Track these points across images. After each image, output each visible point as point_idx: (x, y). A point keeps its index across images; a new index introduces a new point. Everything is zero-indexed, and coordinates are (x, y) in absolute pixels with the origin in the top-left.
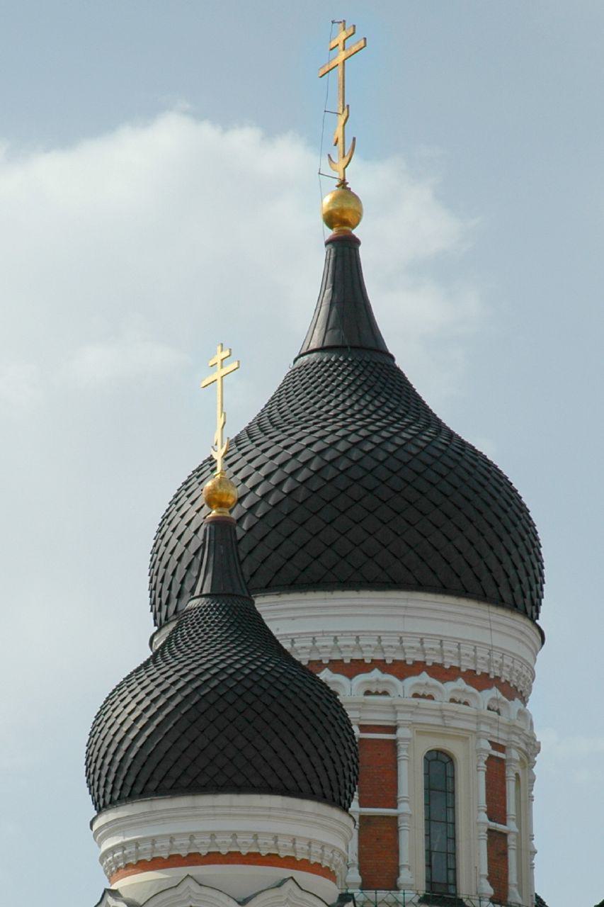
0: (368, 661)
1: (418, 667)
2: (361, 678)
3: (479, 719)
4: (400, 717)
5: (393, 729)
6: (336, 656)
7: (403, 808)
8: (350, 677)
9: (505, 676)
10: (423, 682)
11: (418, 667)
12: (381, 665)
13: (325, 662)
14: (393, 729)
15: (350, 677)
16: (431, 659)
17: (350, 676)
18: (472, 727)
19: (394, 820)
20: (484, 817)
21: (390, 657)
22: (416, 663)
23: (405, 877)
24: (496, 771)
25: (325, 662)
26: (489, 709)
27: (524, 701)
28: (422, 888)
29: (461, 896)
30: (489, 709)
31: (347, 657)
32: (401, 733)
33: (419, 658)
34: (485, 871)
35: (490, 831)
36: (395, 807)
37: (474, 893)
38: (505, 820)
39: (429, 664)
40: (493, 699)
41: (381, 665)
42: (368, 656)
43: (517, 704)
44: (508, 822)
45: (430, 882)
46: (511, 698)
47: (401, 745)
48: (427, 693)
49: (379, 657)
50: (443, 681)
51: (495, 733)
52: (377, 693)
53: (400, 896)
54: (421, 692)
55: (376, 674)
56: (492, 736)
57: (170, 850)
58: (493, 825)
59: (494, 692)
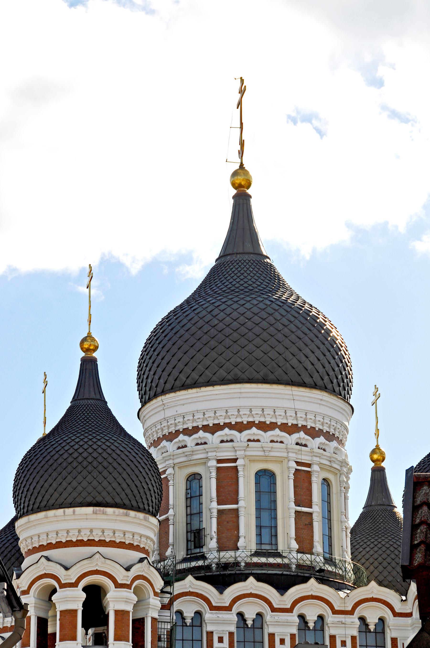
0: (222, 424)
1: (250, 425)
2: (219, 433)
4: (238, 453)
6: (205, 423)
7: (241, 503)
8: (213, 434)
9: (326, 429)
10: (277, 434)
12: (229, 426)
14: (235, 460)
15: (213, 434)
18: (285, 455)
19: (237, 510)
20: (292, 505)
22: (248, 422)
26: (319, 448)
27: (341, 442)
28: (254, 547)
29: (279, 551)
30: (319, 448)
32: (239, 462)
33: (251, 419)
34: (293, 534)
35: (297, 512)
36: (237, 503)
37: (286, 549)
38: (312, 505)
40: (321, 443)
41: (229, 426)
43: (334, 444)
44: (313, 506)
47: (240, 469)
49: (227, 421)
50: (265, 431)
51: (299, 457)
52: (227, 441)
53: (238, 553)
55: (226, 430)
56: (297, 459)
57: (56, 539)
58: (299, 509)
59: (322, 439)
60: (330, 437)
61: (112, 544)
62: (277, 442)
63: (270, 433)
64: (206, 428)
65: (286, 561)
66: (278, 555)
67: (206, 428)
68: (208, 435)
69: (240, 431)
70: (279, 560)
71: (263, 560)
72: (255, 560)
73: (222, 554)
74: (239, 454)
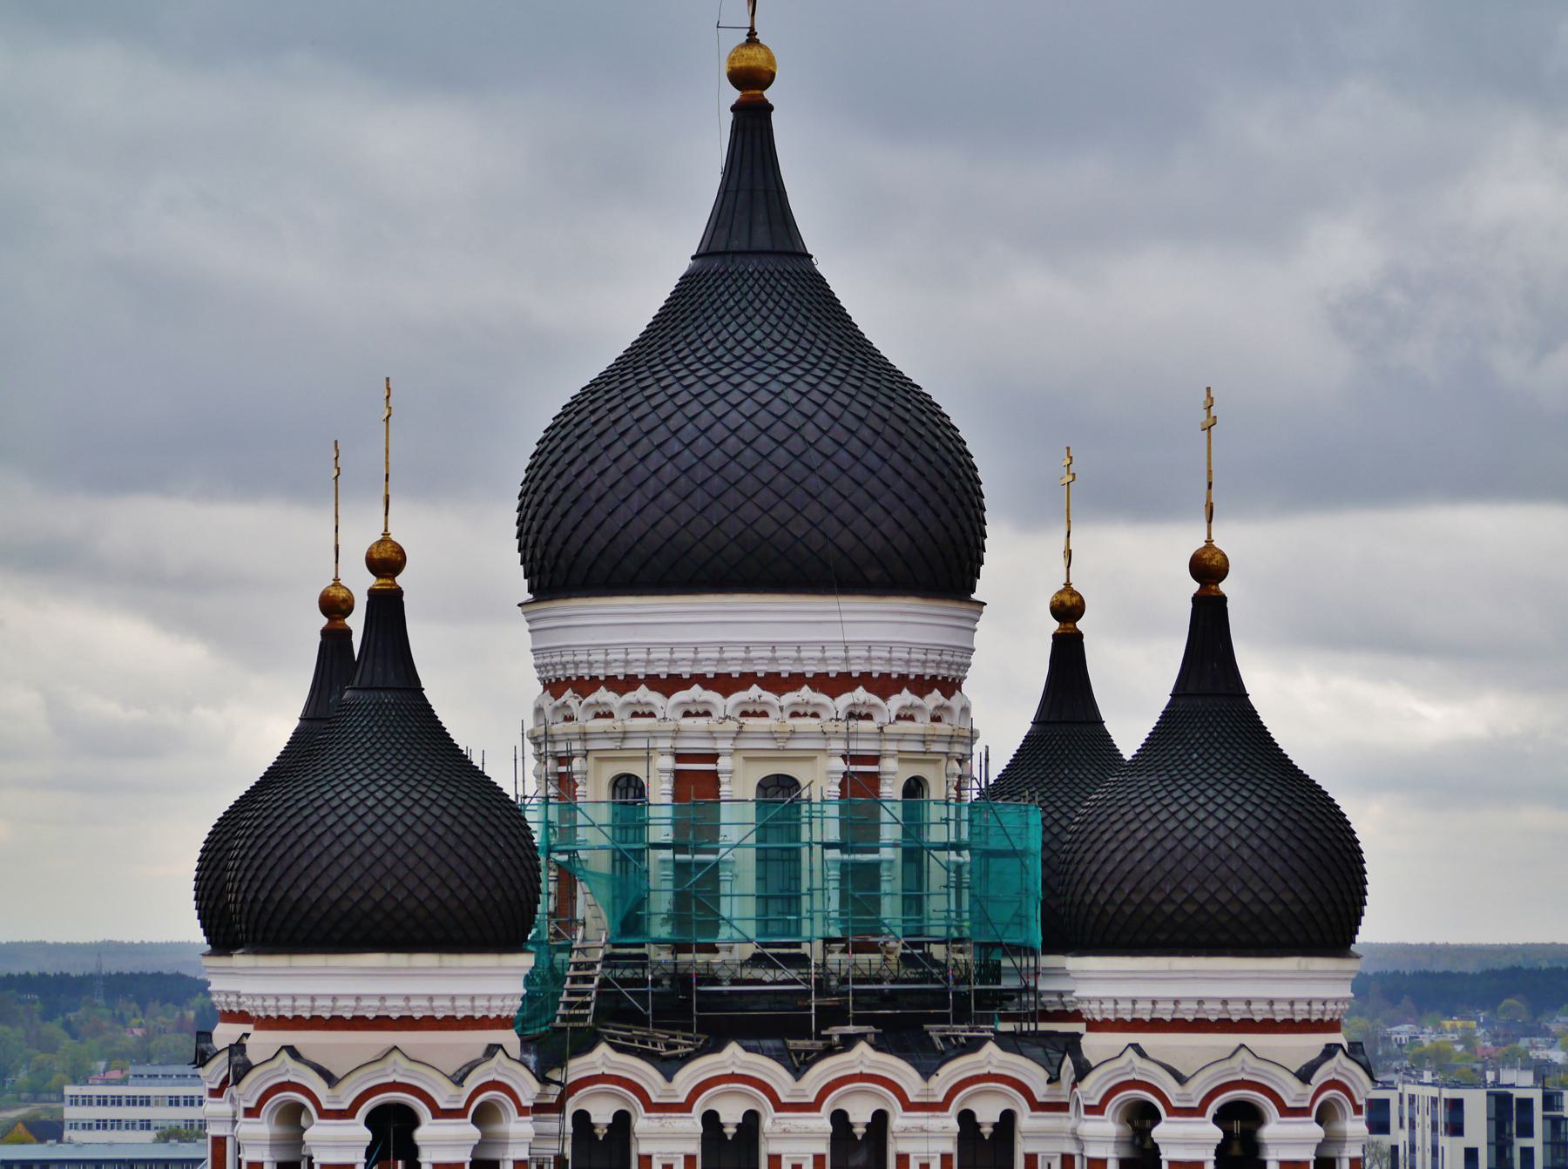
1: (746, 680)
2: (681, 696)
5: (713, 757)
8: (668, 695)
11: (746, 680)
13: (641, 677)
14: (713, 757)
15: (668, 695)
16: (761, 669)
17: (668, 694)
21: (710, 670)
22: (743, 675)
25: (641, 677)
31: (662, 670)
32: (724, 763)
39: (760, 675)
42: (685, 670)
47: (723, 778)
48: (759, 709)
49: (698, 670)
52: (698, 714)
54: (750, 709)
55: (696, 691)
62: (805, 715)
63: (789, 698)
64: (653, 682)
67: (653, 682)
68: (655, 698)
69: (726, 694)
74: (723, 745)
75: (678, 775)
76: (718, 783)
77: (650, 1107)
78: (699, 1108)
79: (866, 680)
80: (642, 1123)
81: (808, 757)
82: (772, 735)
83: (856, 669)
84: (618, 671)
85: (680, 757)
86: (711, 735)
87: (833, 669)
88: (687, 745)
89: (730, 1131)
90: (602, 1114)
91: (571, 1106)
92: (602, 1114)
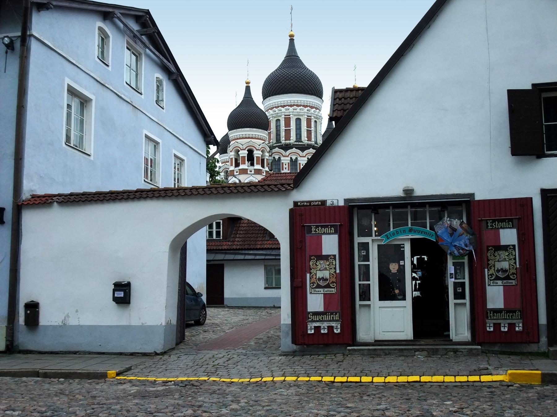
1: (294, 105)
3: (305, 112)
5: (290, 115)
7: (291, 127)
9: (316, 106)
11: (294, 105)
14: (290, 115)
20: (306, 128)
21: (289, 104)
23: (291, 138)
24: (309, 121)
27: (320, 111)
28: (295, 140)
32: (291, 116)
33: (294, 104)
42: (286, 104)
43: (318, 111)
45: (297, 138)
46: (317, 110)
53: (290, 141)
60: (317, 109)
61: (255, 138)
63: (299, 108)
64: (281, 106)
65: (304, 143)
66: (302, 142)
68: (282, 108)
70: (302, 143)
71: (298, 143)
72: (295, 143)
73: (286, 141)
75: (285, 118)
76: (290, 118)
77: (283, 156)
78: (289, 157)
79: (309, 106)
80: (282, 158)
81: (302, 116)
82: (297, 112)
83: (308, 105)
84: (277, 105)
85: (285, 116)
86: (290, 112)
87: (306, 104)
88: (286, 114)
89: (294, 160)
90: (277, 157)
91: (273, 156)
92: (277, 157)
